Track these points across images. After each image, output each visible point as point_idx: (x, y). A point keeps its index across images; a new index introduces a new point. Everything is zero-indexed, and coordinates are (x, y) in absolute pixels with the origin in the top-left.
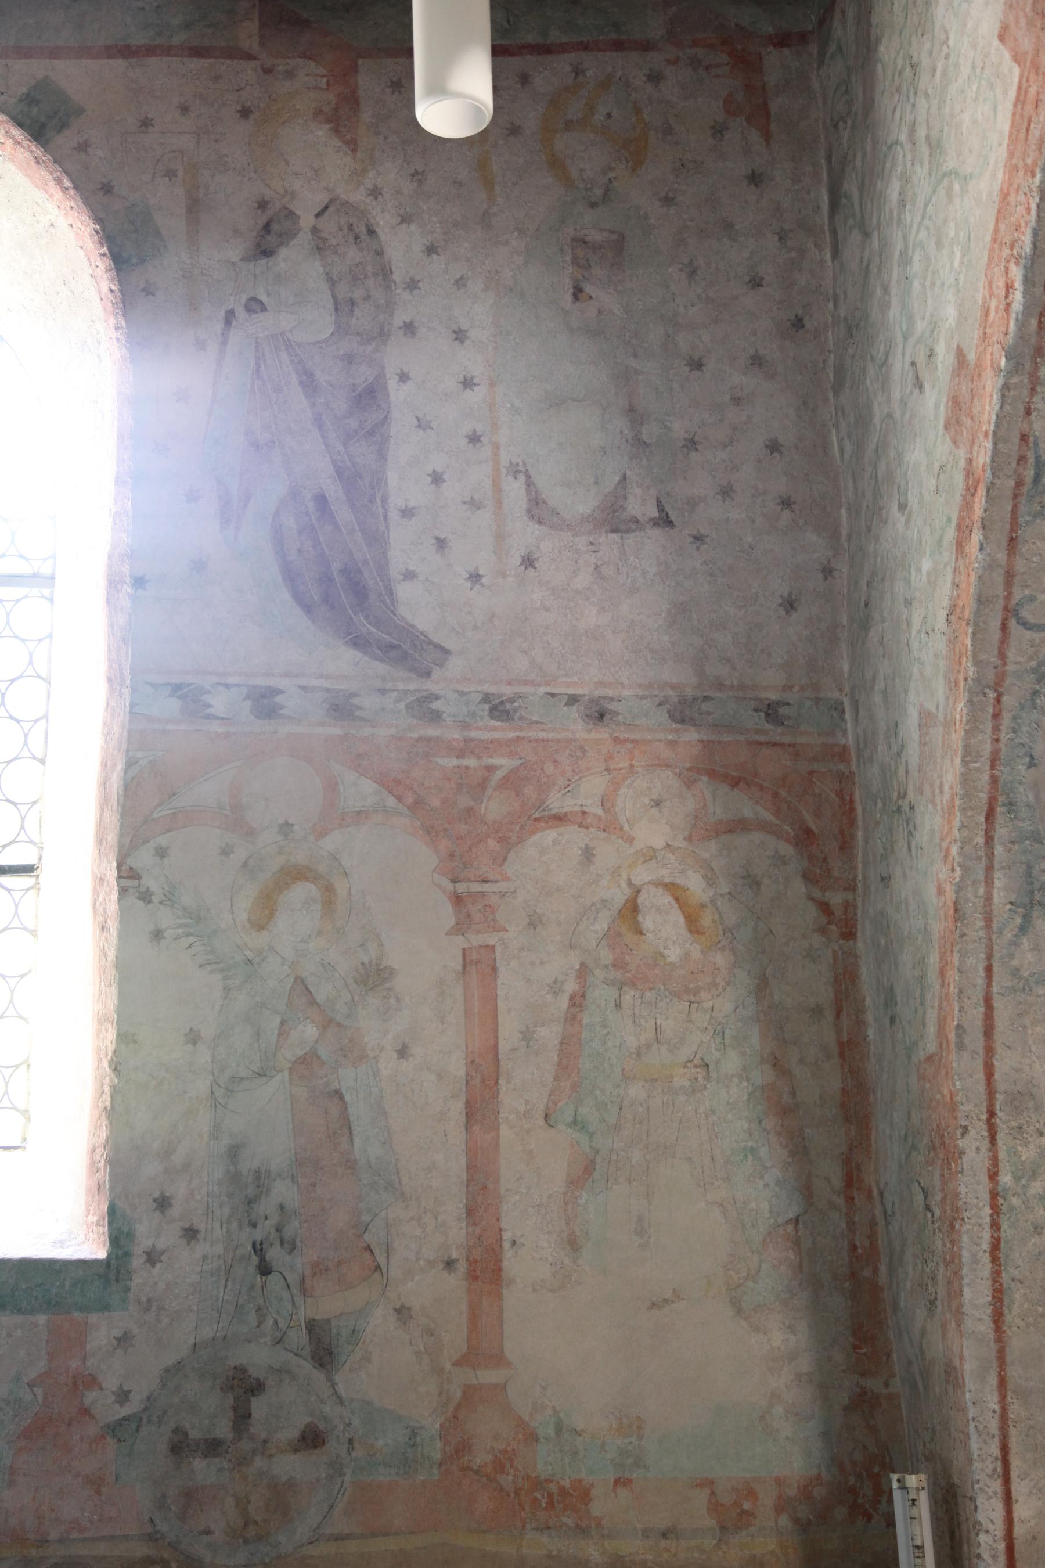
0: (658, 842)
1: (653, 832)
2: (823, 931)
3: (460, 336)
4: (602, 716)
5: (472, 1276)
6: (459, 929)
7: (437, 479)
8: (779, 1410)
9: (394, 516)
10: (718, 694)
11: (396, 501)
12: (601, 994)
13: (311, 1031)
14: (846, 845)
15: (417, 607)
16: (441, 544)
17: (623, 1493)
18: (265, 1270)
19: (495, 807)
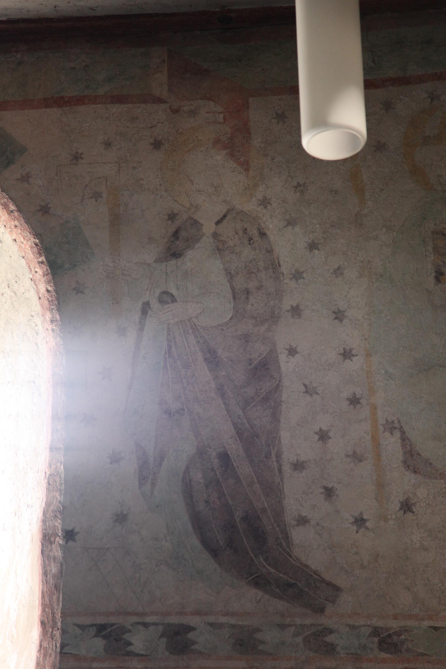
3: (339, 316)
7: (323, 436)
9: (287, 469)
11: (289, 457)
15: (310, 548)
16: (329, 493)
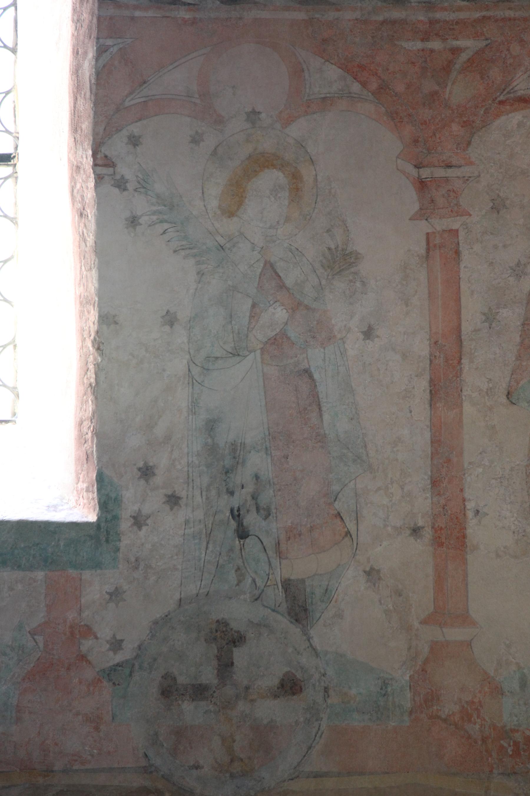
5: (438, 542)
6: (423, 214)
13: (280, 314)
18: (243, 534)
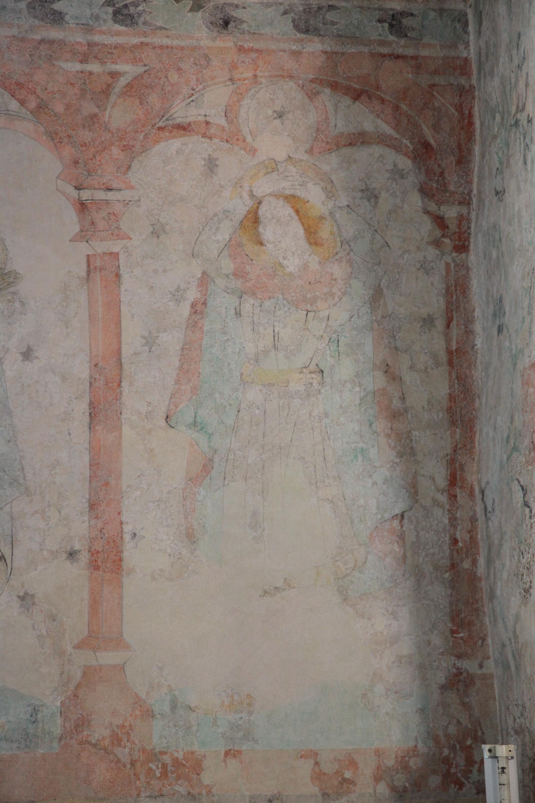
0: (280, 155)
1: (275, 144)
2: (437, 244)
4: (226, 23)
6: (83, 235)
8: (380, 688)
10: (343, 4)
12: (222, 302)
14: (463, 159)
17: (233, 763)
19: (119, 114)
